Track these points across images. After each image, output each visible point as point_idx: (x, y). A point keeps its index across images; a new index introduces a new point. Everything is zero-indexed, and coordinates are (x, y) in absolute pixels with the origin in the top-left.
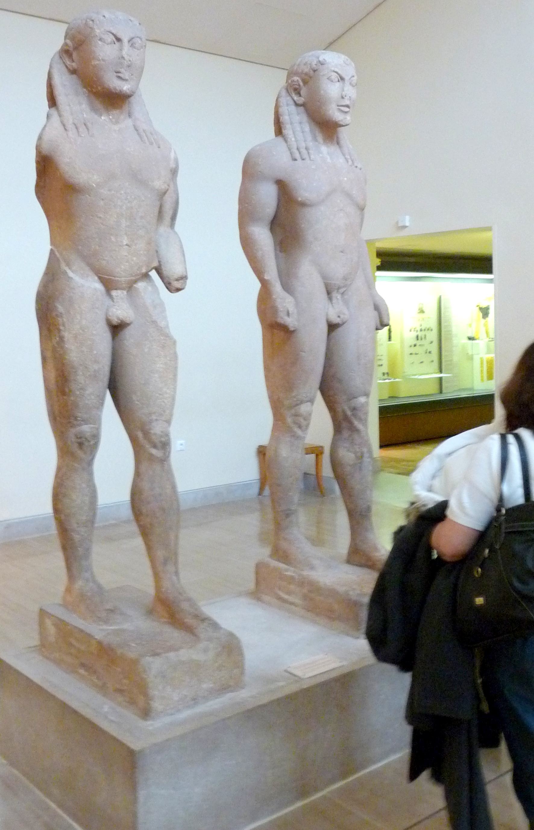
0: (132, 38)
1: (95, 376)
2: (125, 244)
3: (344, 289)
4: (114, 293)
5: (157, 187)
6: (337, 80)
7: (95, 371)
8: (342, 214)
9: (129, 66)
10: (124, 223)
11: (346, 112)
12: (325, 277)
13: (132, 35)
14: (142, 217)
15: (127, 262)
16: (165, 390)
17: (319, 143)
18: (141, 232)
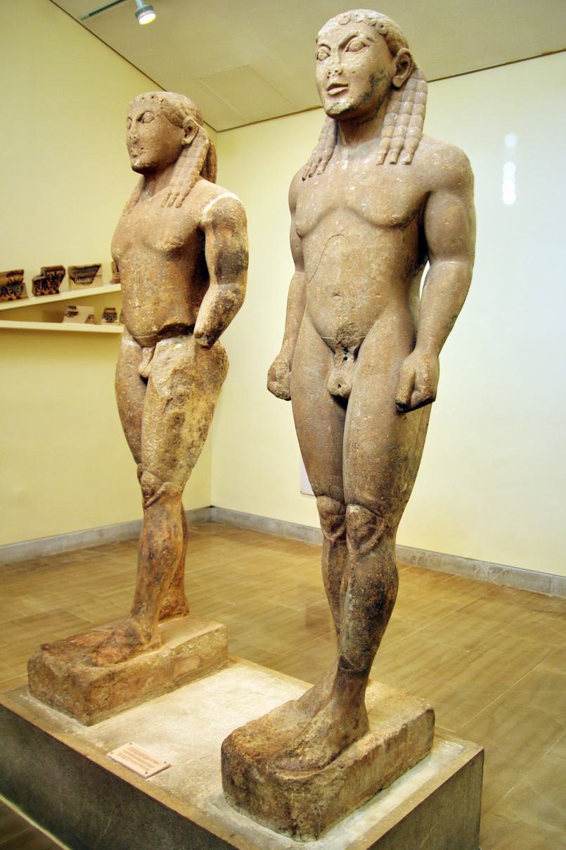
0: (143, 115)
1: (131, 422)
2: (137, 304)
3: (354, 348)
4: (145, 349)
5: (159, 248)
6: (325, 55)
7: (130, 417)
8: (339, 241)
9: (136, 143)
10: (136, 286)
11: (337, 95)
12: (319, 333)
13: (141, 112)
14: (148, 279)
15: (139, 322)
16: (148, 442)
17: (344, 146)
18: (148, 294)
